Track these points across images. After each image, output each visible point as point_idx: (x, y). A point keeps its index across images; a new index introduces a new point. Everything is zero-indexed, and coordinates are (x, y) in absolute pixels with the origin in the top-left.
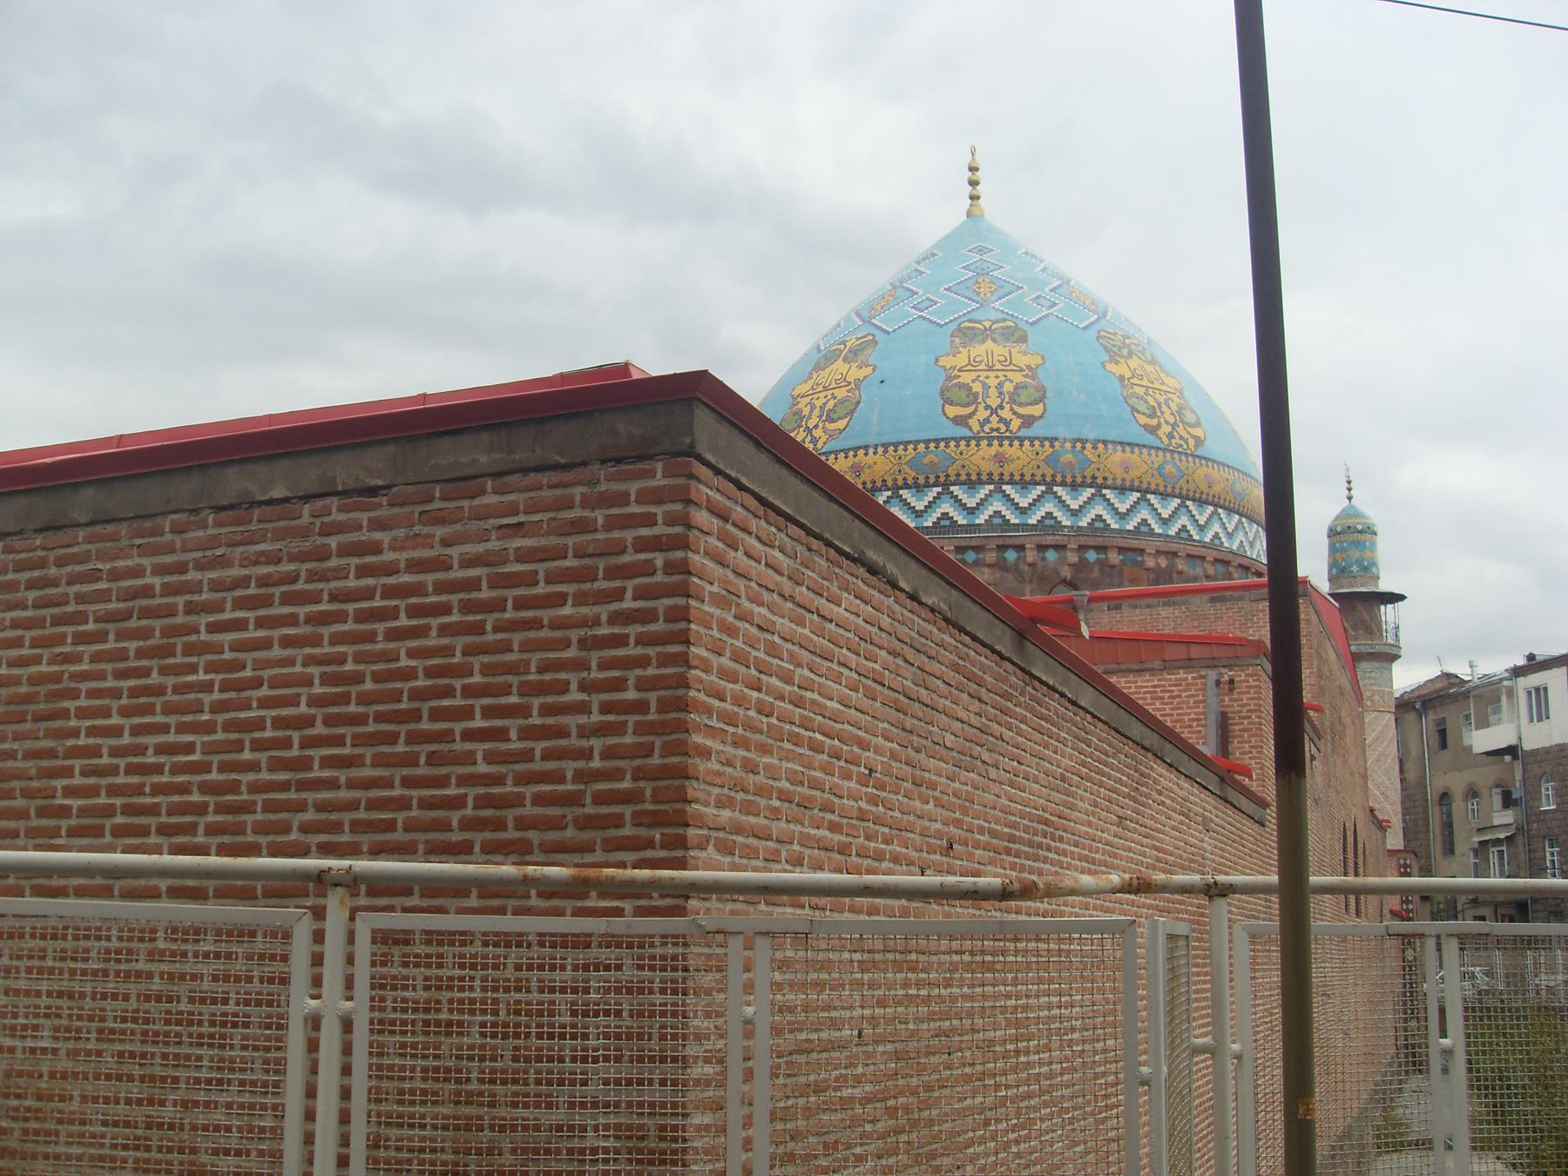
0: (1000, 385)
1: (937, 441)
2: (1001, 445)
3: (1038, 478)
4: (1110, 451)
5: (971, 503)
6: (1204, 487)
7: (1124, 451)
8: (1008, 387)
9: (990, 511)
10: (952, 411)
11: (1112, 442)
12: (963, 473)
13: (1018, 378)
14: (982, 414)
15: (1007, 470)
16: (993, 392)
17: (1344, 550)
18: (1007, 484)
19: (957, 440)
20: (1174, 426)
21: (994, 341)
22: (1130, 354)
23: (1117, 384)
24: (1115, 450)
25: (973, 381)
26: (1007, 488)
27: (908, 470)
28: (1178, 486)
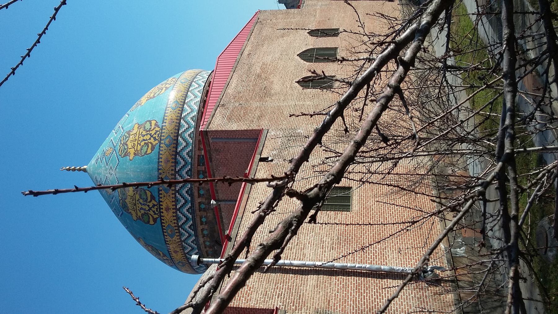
0: (141, 203)
1: (163, 229)
2: (162, 209)
3: (174, 196)
4: (161, 167)
7: (161, 162)
8: (141, 201)
10: (152, 222)
11: (158, 167)
12: (173, 221)
13: (137, 197)
14: (151, 212)
15: (171, 207)
16: (143, 207)
18: (176, 206)
19: (162, 223)
20: (152, 136)
21: (126, 199)
22: (127, 145)
27: (174, 238)
28: (173, 137)
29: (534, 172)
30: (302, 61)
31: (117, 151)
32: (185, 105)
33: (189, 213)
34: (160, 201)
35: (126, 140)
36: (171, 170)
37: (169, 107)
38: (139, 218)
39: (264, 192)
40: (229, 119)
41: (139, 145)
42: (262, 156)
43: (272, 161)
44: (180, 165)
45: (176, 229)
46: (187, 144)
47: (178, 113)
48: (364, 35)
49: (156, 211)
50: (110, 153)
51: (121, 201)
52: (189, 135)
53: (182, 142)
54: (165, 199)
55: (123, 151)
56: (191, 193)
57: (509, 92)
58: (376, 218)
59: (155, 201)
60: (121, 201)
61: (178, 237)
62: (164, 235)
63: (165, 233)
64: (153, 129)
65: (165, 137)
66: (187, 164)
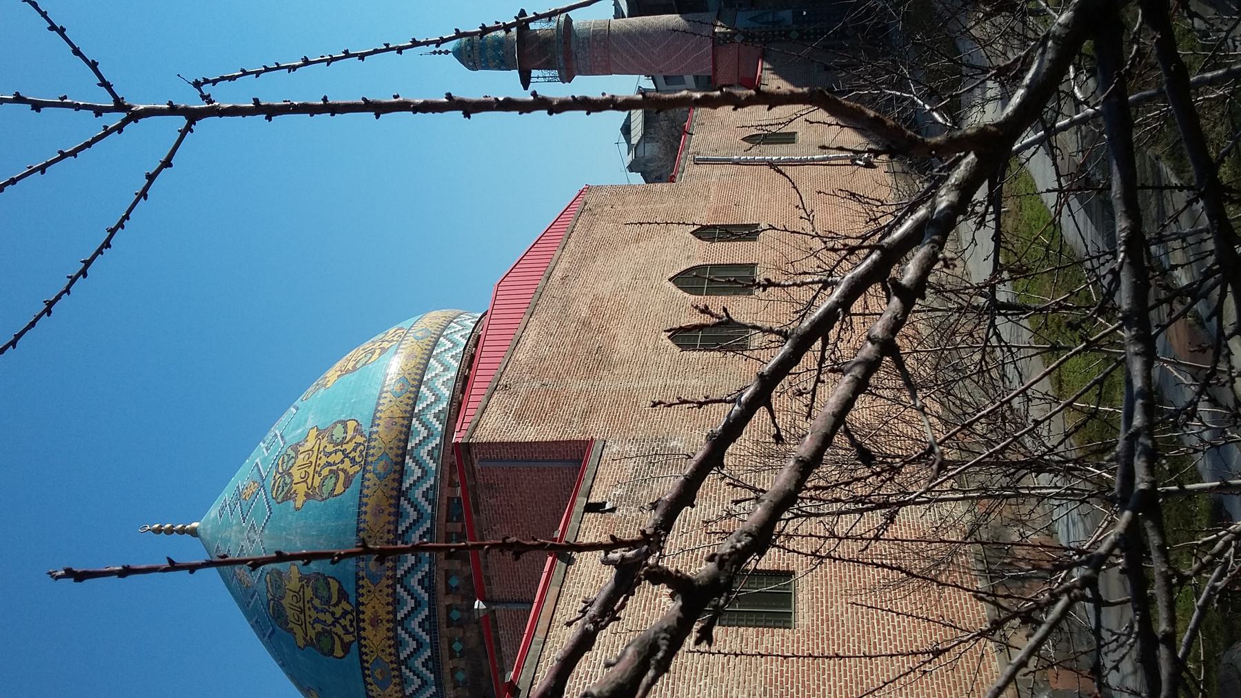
0: (316, 608)
1: (364, 669)
2: (364, 621)
5: (413, 645)
6: (398, 427)
7: (365, 513)
8: (317, 602)
9: (419, 630)
10: (339, 652)
11: (358, 524)
12: (388, 650)
13: (309, 593)
15: (384, 616)
16: (321, 616)
17: (487, 60)
18: (395, 616)
19: (361, 654)
20: (346, 456)
21: (282, 598)
22: (290, 475)
23: (311, 501)
24: (365, 521)
25: (314, 629)
26: (400, 616)
27: (389, 690)
29: (1205, 539)
30: (680, 291)
31: (269, 489)
32: (423, 387)
33: (423, 631)
34: (359, 604)
35: (290, 465)
36: (386, 531)
37: (387, 392)
38: (310, 643)
39: (594, 583)
40: (520, 417)
41: (316, 475)
42: (592, 500)
43: (613, 510)
44: (407, 520)
45: (393, 669)
46: (425, 473)
47: (407, 405)
48: (814, 237)
49: (348, 627)
50: (253, 493)
51: (272, 602)
52: (430, 453)
53: (412, 468)
54: (370, 598)
55: (280, 489)
56: (430, 584)
57: (1136, 354)
58: (851, 645)
59: (348, 602)
60: (272, 602)
61: (398, 688)
62: (365, 682)
63: (367, 679)
64: (351, 440)
65: (375, 458)
66: (422, 518)
